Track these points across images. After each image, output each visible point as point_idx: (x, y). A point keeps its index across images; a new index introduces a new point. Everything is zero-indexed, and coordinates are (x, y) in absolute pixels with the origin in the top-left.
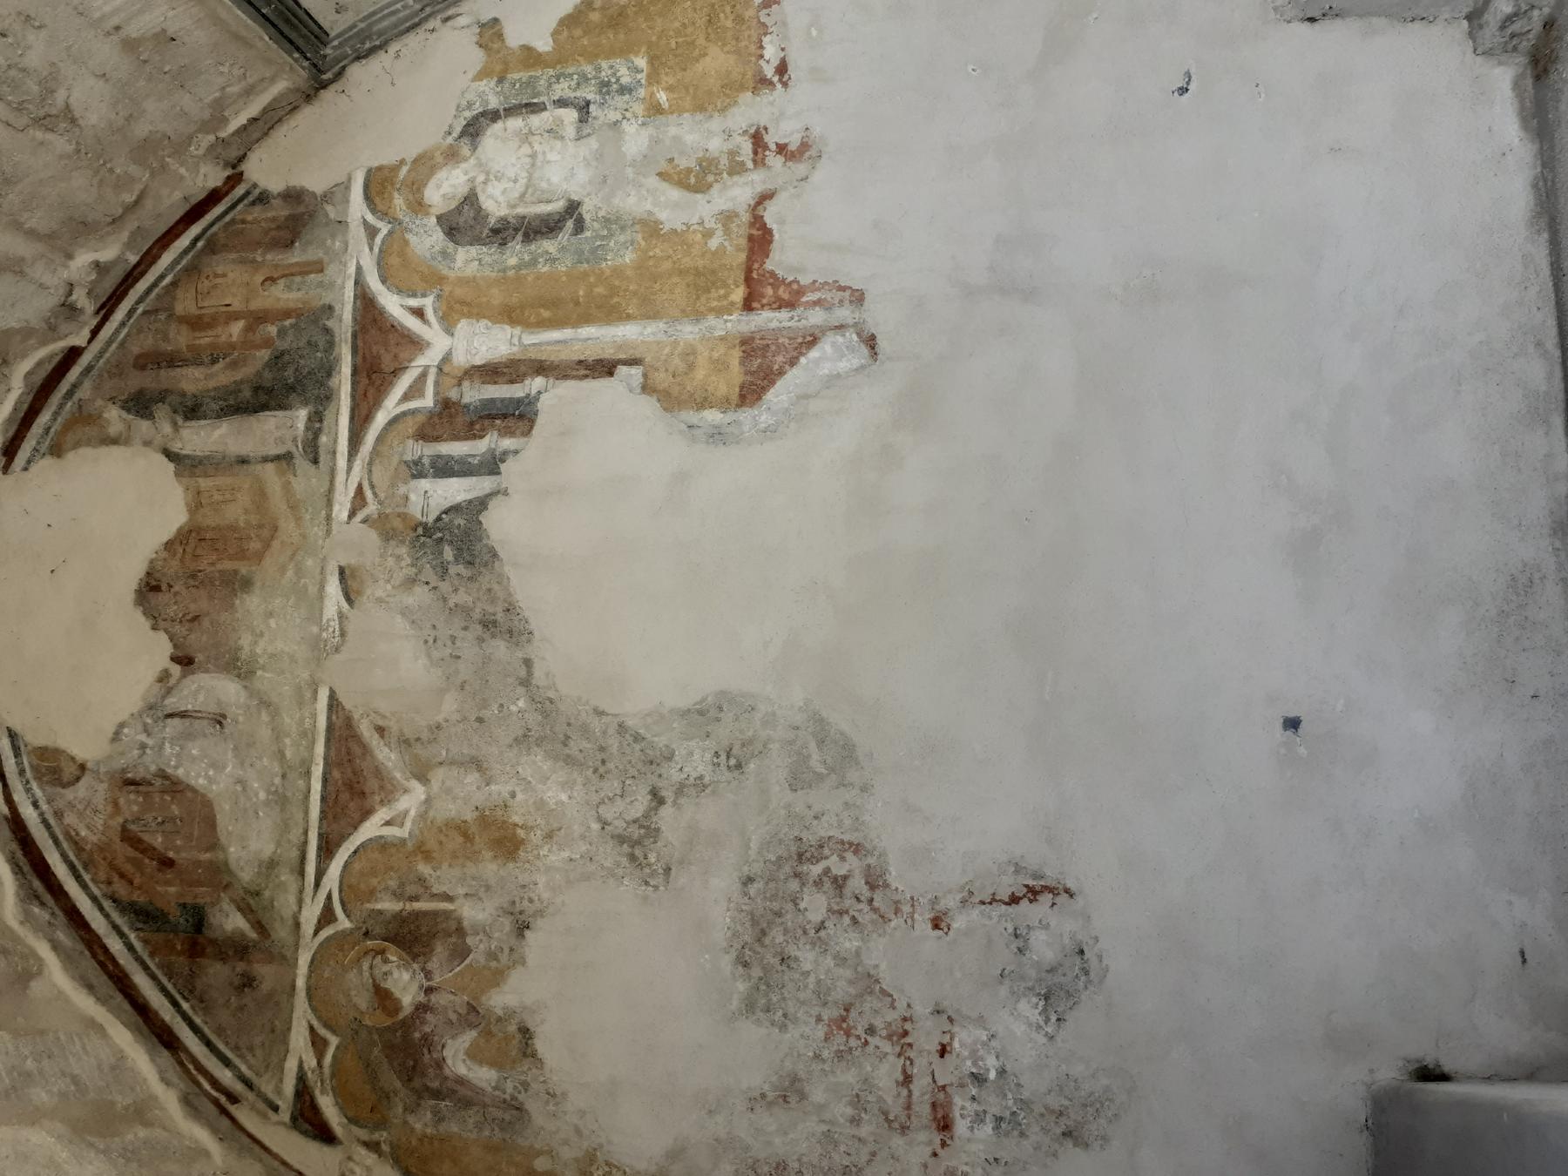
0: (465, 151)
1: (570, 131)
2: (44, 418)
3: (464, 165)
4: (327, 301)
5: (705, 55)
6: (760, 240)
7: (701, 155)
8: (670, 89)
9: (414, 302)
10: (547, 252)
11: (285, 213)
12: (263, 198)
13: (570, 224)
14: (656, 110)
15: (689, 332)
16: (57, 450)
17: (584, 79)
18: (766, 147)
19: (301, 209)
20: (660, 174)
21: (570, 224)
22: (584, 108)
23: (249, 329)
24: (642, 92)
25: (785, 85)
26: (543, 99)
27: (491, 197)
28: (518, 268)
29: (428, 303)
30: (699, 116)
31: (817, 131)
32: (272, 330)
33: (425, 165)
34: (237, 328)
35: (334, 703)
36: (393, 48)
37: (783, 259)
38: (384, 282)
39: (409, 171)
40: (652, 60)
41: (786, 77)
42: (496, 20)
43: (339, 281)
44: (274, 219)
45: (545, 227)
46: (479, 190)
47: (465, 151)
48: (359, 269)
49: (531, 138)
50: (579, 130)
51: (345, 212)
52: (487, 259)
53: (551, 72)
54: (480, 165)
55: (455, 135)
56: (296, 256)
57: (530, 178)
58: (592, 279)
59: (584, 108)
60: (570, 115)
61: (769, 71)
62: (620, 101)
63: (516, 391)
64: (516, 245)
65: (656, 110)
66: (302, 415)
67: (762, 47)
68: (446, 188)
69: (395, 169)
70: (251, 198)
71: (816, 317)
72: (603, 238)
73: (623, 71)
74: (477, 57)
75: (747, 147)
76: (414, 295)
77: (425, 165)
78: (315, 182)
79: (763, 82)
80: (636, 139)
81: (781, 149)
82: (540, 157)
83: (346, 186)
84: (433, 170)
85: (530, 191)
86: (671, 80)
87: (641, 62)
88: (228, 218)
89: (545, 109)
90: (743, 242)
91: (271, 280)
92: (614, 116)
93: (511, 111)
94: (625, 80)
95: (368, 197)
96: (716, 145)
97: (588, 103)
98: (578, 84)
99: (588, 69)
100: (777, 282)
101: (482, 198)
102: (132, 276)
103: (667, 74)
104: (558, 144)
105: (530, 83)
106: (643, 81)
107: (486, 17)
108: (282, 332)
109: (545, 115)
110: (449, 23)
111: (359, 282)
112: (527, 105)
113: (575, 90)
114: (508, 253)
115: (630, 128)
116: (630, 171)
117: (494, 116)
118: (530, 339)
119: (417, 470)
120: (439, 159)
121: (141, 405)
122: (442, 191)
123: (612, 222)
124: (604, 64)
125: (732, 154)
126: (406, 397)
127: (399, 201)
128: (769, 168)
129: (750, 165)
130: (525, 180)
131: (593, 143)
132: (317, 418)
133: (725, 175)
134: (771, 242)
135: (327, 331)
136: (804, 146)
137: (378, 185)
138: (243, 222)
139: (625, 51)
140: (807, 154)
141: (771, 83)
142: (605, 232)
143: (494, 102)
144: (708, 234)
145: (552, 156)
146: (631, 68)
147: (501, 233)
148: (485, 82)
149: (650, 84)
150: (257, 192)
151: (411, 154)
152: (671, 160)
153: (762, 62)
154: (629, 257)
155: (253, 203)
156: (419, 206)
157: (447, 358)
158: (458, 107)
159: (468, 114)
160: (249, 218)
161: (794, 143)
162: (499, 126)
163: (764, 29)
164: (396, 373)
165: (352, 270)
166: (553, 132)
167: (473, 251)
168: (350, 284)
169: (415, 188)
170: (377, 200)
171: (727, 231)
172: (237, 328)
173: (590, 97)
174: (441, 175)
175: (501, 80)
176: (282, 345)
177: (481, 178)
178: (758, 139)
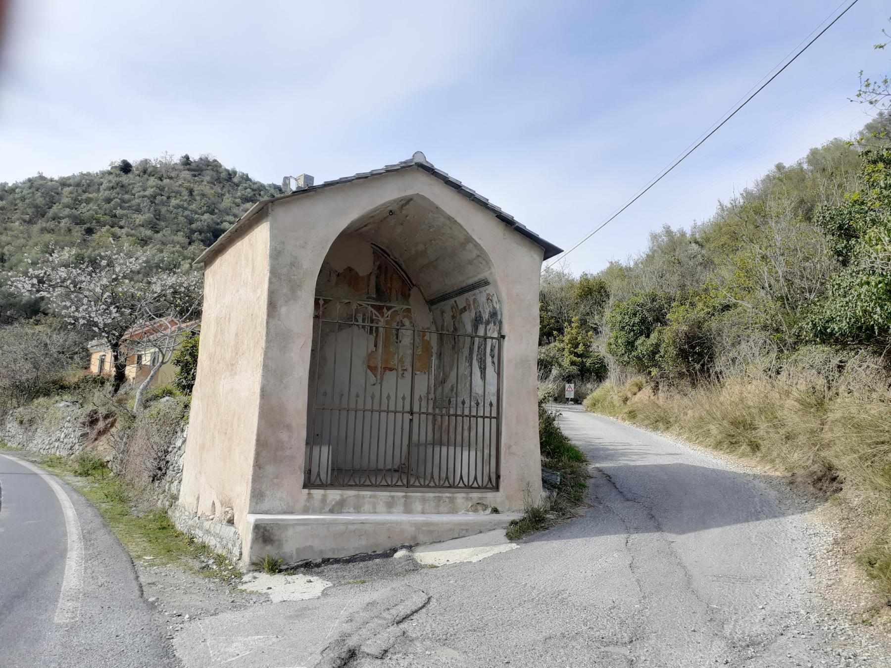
2: (379, 250)
6: (391, 370)
12: (410, 290)
15: (379, 358)
16: (373, 253)
17: (419, 344)
32: (388, 291)
33: (410, 318)
34: (389, 285)
35: (330, 300)
37: (388, 373)
56: (399, 295)
63: (374, 331)
64: (396, 332)
66: (375, 296)
71: (379, 377)
78: (411, 300)
96: (406, 364)
100: (384, 372)
102: (400, 267)
111: (394, 307)
118: (381, 334)
119: (364, 315)
121: (380, 267)
123: (398, 348)
126: (375, 314)
132: (374, 299)
137: (408, 310)
154: (391, 350)
156: (404, 317)
157: (380, 321)
161: (404, 375)
164: (379, 313)
176: (386, 293)
178: (406, 370)
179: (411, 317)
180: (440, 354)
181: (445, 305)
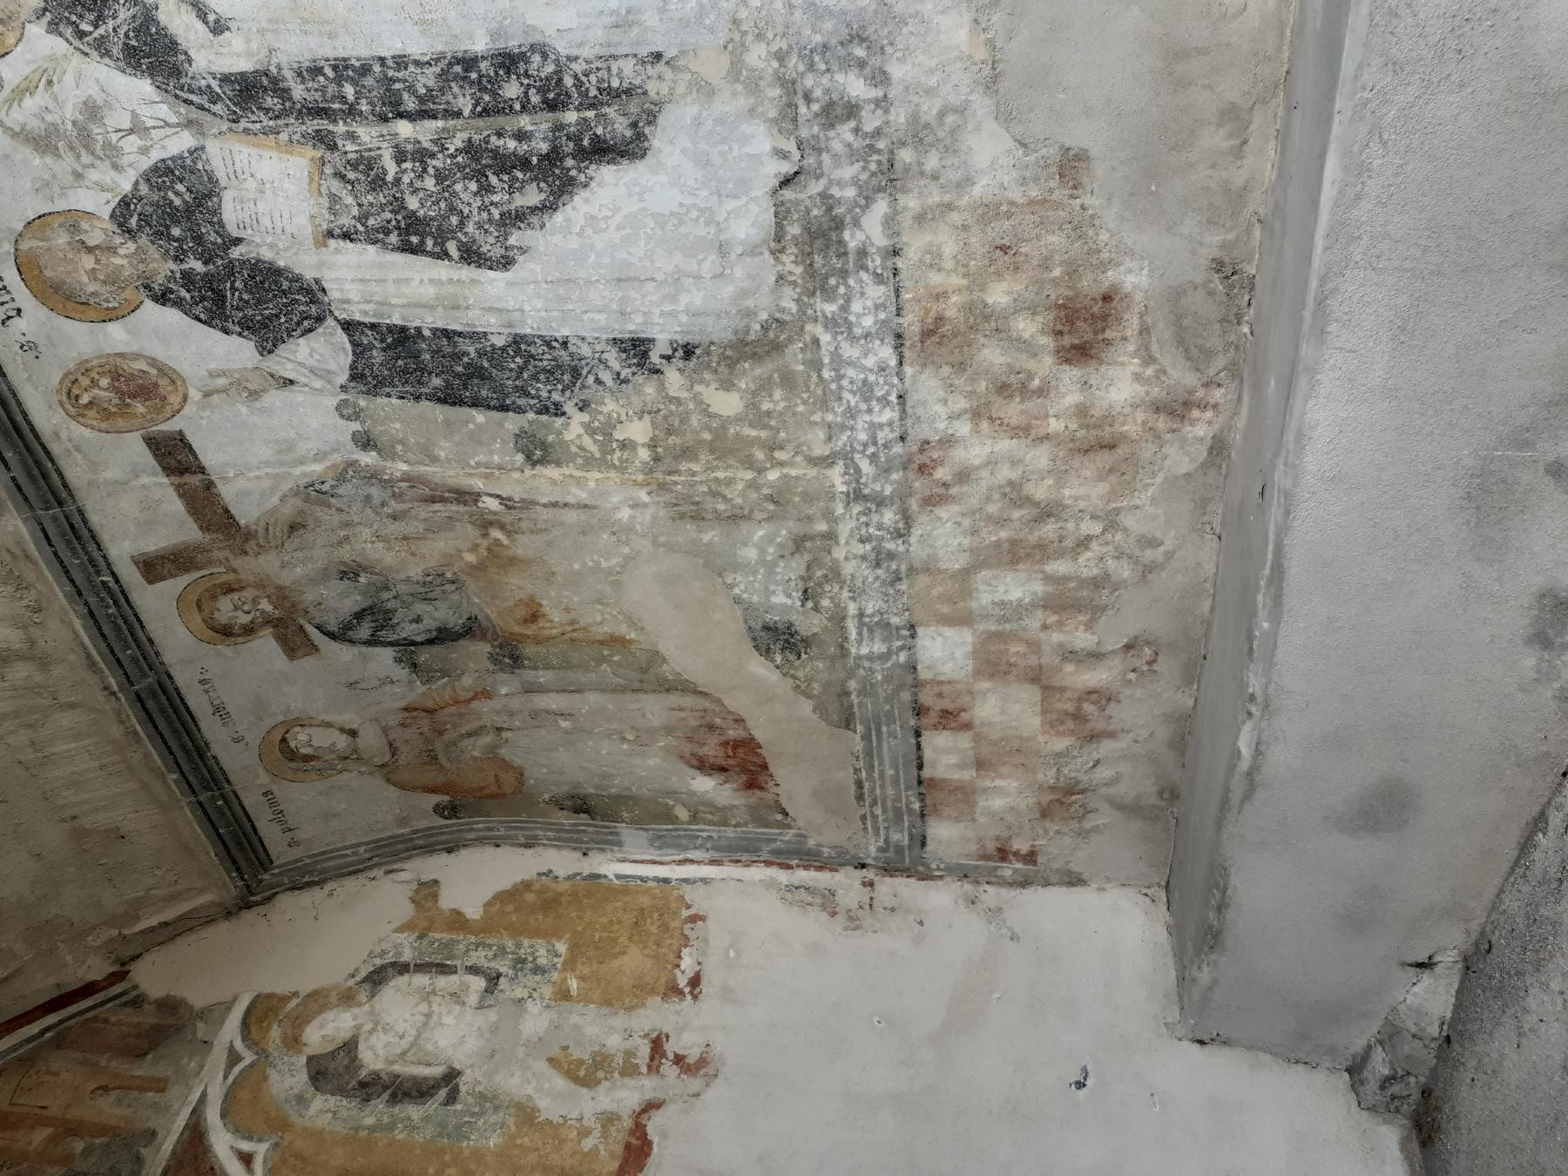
0: (363, 997)
1: (473, 999)
3: (356, 1011)
4: (150, 1125)
5: (624, 953)
7: (597, 1049)
8: (582, 978)
9: (246, 1146)
10: (409, 1119)
11: (153, 1021)
12: (138, 1002)
13: (443, 1093)
14: (564, 995)
17: (502, 951)
18: (664, 1055)
19: (171, 1021)
20: (551, 1061)
21: (443, 1093)
22: (493, 979)
23: (52, 1139)
24: (555, 976)
25: (695, 997)
26: (457, 962)
27: (372, 1048)
28: (372, 1129)
29: (260, 1150)
30: (605, 1011)
31: (718, 1049)
32: (79, 1145)
33: (317, 1002)
34: (40, 1136)
36: (329, 887)
38: (223, 1116)
39: (298, 1005)
40: (574, 948)
41: (697, 990)
42: (436, 882)
43: (176, 1107)
44: (138, 1025)
45: (417, 1091)
46: (361, 1039)
47: (363, 997)
48: (204, 1095)
49: (432, 998)
50: (482, 999)
51: (215, 1033)
52: (343, 1113)
53: (473, 939)
54: (372, 1013)
55: (358, 979)
56: (141, 1069)
57: (418, 1037)
58: (447, 1158)
59: (493, 979)
60: (479, 983)
61: (682, 982)
62: (532, 980)
64: (379, 1104)
65: (564, 995)
67: (680, 957)
68: (329, 1030)
69: (285, 999)
70: (124, 999)
72: (473, 1114)
73: (542, 952)
74: (407, 911)
75: (645, 1050)
76: (250, 1138)
77: (317, 1002)
78: (197, 998)
79: (673, 991)
80: (535, 1020)
81: (679, 1059)
82: (435, 1018)
83: (228, 1006)
84: (324, 1008)
85: (413, 1051)
86: (586, 970)
87: (562, 947)
88: (90, 1015)
89: (456, 972)
90: (619, 1149)
91: (105, 1089)
92: (520, 993)
93: (421, 968)
94: (542, 961)
95: (245, 1024)
96: (614, 1042)
97: (499, 976)
98: (495, 955)
99: (510, 944)
101: (361, 1047)
103: (583, 964)
104: (457, 1008)
105: (448, 946)
106: (559, 966)
107: (426, 877)
108: (88, 1151)
109: (454, 978)
110: (391, 876)
111: (198, 1112)
112: (438, 965)
113: (490, 961)
114: (368, 1110)
115: (533, 1008)
116: (520, 1052)
117: (403, 968)
120: (333, 999)
122: (324, 1032)
123: (489, 1100)
124: (526, 943)
125: (629, 1054)
127: (275, 1033)
128: (663, 1076)
129: (644, 1069)
130: (411, 1039)
131: (493, 1015)
133: (616, 1075)
134: (648, 1155)
135: (139, 1160)
136: (702, 1062)
137: (262, 1012)
138: (106, 1021)
139: (549, 934)
140: (703, 1072)
141: (681, 993)
142: (477, 1109)
143: (407, 956)
144: (585, 1133)
145: (448, 1020)
146: (550, 951)
147: (369, 1088)
148: (406, 934)
149: (564, 969)
150: (135, 993)
151: (306, 988)
152: (565, 1048)
153: (677, 971)
154: (494, 1141)
155: (125, 1005)
156: (293, 1042)
158: (371, 952)
159: (378, 962)
160: (113, 1019)
161: (693, 1055)
162: (403, 980)
163: (686, 941)
165: (195, 1096)
166: (456, 997)
167: (332, 1101)
168: (187, 1111)
169: (300, 1021)
170: (254, 1028)
171: (605, 1134)
172: (40, 1136)
173: (503, 970)
174: (329, 1015)
175: (420, 937)
177: (368, 1027)
178: (657, 1045)
179: (314, 995)
180: (581, 805)
181: (219, 710)
